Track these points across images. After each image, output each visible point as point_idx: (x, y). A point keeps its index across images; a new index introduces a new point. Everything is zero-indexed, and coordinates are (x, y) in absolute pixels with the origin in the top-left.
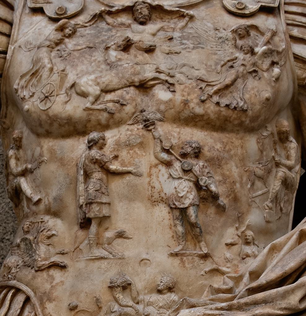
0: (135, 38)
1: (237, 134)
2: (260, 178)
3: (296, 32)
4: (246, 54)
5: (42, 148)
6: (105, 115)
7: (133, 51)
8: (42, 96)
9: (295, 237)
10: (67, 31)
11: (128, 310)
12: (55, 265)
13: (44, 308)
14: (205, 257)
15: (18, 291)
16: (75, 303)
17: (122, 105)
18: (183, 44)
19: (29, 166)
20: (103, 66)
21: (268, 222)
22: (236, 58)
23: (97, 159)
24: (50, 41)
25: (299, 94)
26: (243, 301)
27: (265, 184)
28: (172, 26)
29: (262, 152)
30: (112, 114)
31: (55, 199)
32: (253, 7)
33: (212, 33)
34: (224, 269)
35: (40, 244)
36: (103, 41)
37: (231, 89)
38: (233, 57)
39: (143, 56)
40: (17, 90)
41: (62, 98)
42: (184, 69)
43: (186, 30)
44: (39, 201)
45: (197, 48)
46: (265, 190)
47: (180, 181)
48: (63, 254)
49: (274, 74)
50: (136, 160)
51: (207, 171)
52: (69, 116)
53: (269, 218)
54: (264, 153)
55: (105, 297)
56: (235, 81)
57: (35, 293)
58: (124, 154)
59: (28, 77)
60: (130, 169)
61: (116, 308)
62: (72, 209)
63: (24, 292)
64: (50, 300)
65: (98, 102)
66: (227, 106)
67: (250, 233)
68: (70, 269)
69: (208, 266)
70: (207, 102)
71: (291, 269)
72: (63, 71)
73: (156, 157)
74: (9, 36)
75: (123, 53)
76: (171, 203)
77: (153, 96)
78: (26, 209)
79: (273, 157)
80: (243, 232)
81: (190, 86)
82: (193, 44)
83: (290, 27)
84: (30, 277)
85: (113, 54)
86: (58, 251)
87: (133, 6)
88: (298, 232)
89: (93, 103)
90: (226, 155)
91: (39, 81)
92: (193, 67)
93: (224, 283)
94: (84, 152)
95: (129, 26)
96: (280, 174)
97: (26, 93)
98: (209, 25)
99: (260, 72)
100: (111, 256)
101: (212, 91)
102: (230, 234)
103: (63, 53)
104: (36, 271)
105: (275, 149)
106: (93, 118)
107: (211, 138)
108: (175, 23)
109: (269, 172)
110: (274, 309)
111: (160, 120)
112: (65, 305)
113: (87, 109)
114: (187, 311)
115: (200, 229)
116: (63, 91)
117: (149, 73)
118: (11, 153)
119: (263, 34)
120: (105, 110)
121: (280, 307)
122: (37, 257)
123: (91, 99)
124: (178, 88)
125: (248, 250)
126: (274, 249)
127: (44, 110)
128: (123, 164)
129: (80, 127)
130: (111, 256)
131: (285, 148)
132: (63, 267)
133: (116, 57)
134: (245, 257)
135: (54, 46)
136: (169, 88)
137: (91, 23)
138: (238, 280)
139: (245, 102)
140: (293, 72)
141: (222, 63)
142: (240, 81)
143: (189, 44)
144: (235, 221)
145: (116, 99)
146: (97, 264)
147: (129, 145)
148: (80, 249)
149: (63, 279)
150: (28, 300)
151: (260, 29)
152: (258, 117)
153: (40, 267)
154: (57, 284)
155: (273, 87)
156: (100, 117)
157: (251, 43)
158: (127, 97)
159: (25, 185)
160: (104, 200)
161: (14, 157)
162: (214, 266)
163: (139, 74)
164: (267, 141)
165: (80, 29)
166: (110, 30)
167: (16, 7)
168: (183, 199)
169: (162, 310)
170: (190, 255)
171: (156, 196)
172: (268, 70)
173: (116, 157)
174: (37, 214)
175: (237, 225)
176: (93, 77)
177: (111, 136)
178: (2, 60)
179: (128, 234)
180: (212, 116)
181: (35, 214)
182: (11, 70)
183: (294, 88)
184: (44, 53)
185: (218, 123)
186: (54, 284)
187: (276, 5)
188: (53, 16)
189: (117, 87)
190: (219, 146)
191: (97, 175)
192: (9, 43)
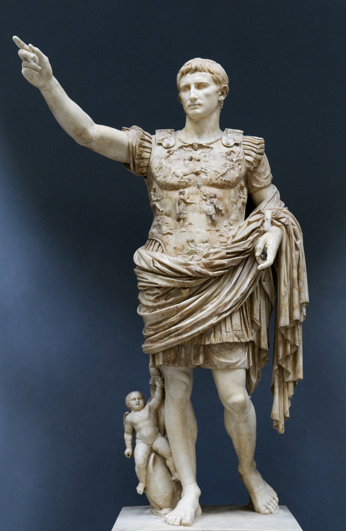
0: (194, 156)
1: (228, 189)
3: (246, 152)
4: (230, 161)
5: (163, 193)
6: (185, 183)
7: (193, 160)
8: (164, 176)
9: (246, 224)
10: (171, 153)
12: (169, 233)
13: (165, 248)
14: (217, 231)
15: (156, 241)
16: (176, 246)
17: (190, 180)
18: (209, 158)
19: (159, 199)
20: (184, 166)
21: (237, 217)
22: (227, 163)
23: (182, 199)
24: (165, 156)
25: (247, 172)
26: (230, 246)
27: (236, 205)
28: (206, 151)
29: (235, 194)
30: (187, 183)
31: (168, 211)
33: (219, 154)
34: (224, 234)
35: (163, 226)
36: (183, 157)
37: (225, 175)
38: (226, 163)
39: (196, 162)
40: (154, 173)
41: (170, 177)
42: (210, 167)
43: (210, 153)
44: (163, 211)
45: (214, 159)
46: (236, 207)
47: (210, 206)
48: (171, 229)
49: (239, 168)
50: (195, 199)
51: (218, 202)
52: (173, 183)
53: (238, 216)
54: (236, 194)
55: (185, 244)
56: (227, 171)
57: (162, 242)
58: (191, 197)
59: (158, 169)
60: (193, 202)
61: (189, 248)
62: (174, 214)
63: (158, 242)
64: (167, 245)
65: (182, 179)
66: (225, 181)
67: (232, 222)
68: (174, 235)
69: (219, 234)
70: (218, 179)
71: (245, 235)
72: (170, 168)
73: (202, 198)
74: (151, 153)
75: (190, 161)
76: (207, 213)
77: (200, 177)
78: (157, 212)
79: (239, 195)
80: (230, 222)
81: (212, 174)
82: (213, 158)
83: (244, 150)
84: (160, 237)
85: (187, 162)
86: (170, 228)
87: (193, 144)
88: (247, 222)
89: (181, 179)
90: (224, 197)
91: (162, 171)
92: (213, 167)
93: (224, 240)
94: (178, 196)
95: (191, 151)
96: (241, 201)
97: (157, 175)
98: (219, 151)
99: (235, 168)
100: (187, 231)
101: (220, 175)
102: (226, 223)
103: (170, 161)
104: (163, 235)
105: (240, 192)
106: (181, 184)
107: (219, 191)
108: (206, 150)
109: (238, 200)
110: (240, 248)
111: (203, 185)
112: (173, 246)
113: (179, 182)
114: (213, 249)
115: (216, 221)
116: (170, 175)
117: (198, 169)
118: (152, 193)
119: (235, 153)
120: (185, 182)
121: (242, 248)
122: (163, 230)
123: (180, 178)
124: (208, 174)
125: (231, 227)
126: (240, 227)
127: (164, 181)
128: (191, 200)
129: (176, 187)
130: (187, 231)
131: (243, 191)
132: (171, 234)
133: (188, 163)
135: (166, 157)
136: (205, 174)
137: (178, 150)
138: (228, 238)
139: (230, 179)
140: (245, 166)
141: (223, 165)
142: (228, 171)
143: (211, 158)
144: (227, 218)
145: (188, 178)
146: (183, 233)
147: (193, 194)
148: (177, 228)
149: (172, 238)
150: (160, 244)
151: (235, 152)
152: (234, 183)
153: (164, 234)
154: (169, 240)
155: (239, 173)
156: (183, 184)
157: (232, 158)
158: (192, 177)
159: (158, 205)
160: (185, 212)
161: (153, 195)
162: (221, 234)
163: (195, 169)
164: (237, 190)
165: (175, 152)
166: (185, 153)
167: (152, 143)
168: (210, 212)
169: (204, 249)
170: (213, 230)
171: (202, 211)
172: (237, 167)
173: (188, 198)
174: (162, 215)
175: (228, 219)
176: (180, 170)
177: (187, 190)
178: (149, 161)
179: (192, 224)
180: (220, 184)
181: (161, 215)
182: (152, 165)
183: (246, 171)
185: (221, 186)
186: (169, 239)
187: (240, 143)
188: (166, 147)
189: (188, 174)
190: (222, 194)
191: (183, 204)
192: (151, 156)
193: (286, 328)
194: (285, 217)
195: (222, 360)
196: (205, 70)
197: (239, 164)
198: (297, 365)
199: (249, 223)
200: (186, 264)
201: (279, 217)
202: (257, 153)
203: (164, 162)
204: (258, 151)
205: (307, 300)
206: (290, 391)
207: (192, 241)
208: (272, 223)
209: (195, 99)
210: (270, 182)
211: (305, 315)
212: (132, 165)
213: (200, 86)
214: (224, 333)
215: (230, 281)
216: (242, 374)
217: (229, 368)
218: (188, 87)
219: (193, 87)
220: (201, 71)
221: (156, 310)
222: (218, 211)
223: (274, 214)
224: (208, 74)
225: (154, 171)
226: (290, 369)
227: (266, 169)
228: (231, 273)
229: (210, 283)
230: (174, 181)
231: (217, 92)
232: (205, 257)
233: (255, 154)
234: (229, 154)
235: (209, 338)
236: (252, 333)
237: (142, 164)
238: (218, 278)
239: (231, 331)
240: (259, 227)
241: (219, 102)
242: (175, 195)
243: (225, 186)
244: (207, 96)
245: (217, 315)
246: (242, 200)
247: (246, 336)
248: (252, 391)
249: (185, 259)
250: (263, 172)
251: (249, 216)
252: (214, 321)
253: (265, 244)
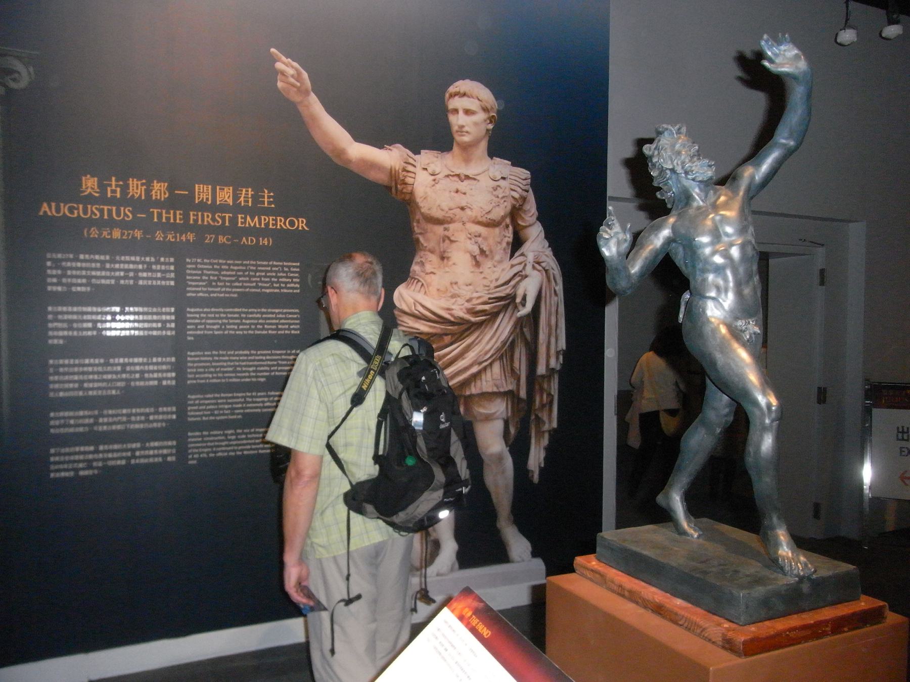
0: (460, 188)
2: (499, 243)
3: (513, 187)
7: (459, 193)
11: (457, 292)
14: (481, 273)
15: (415, 279)
30: (452, 219)
34: (487, 277)
55: (448, 284)
61: (452, 290)
69: (483, 276)
109: (502, 240)
117: (464, 204)
120: (450, 217)
125: (495, 269)
126: (503, 270)
134: (494, 272)
177: (452, 226)
190: (486, 233)
191: (447, 241)
193: (543, 376)
195: (482, 410)
197: (505, 201)
198: (552, 414)
200: (448, 309)
202: (523, 190)
204: (524, 188)
205: (564, 348)
206: (545, 441)
207: (456, 283)
209: (463, 127)
210: (535, 219)
211: (562, 362)
213: (468, 112)
214: (484, 383)
215: (492, 327)
216: (499, 425)
217: (488, 418)
218: (456, 111)
219: (461, 112)
220: (469, 97)
222: (482, 252)
226: (545, 418)
227: (531, 207)
229: (472, 329)
230: (438, 214)
231: (485, 121)
232: (468, 301)
233: (521, 190)
234: (495, 189)
235: (470, 389)
236: (511, 382)
238: (479, 325)
239: (491, 380)
241: (488, 130)
243: (491, 224)
246: (506, 239)
247: (505, 385)
248: (510, 443)
250: (529, 210)
251: (514, 255)
252: (475, 369)
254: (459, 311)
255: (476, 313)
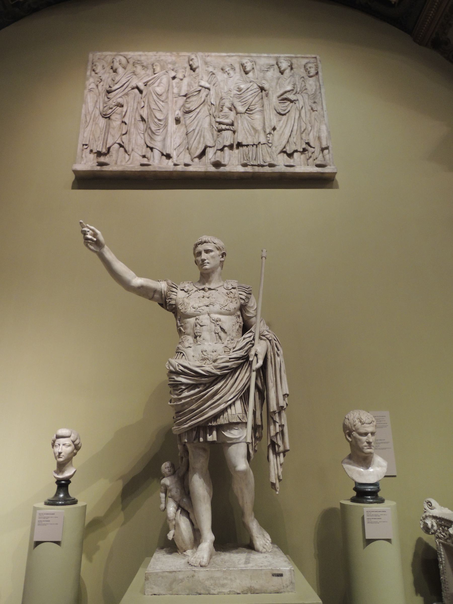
10: (190, 294)
11: (206, 357)
14: (223, 343)
15: (181, 353)
32: (230, 287)
41: (189, 309)
61: (203, 356)
109: (236, 324)
116: (189, 307)
125: (232, 341)
130: (201, 344)
138: (230, 349)
151: (233, 292)
159: (182, 329)
177: (201, 317)
184: (185, 299)
188: (186, 291)
191: (198, 326)
194: (269, 334)
196: (210, 241)
199: (244, 339)
201: (265, 334)
202: (247, 294)
203: (185, 299)
208: (261, 339)
209: (205, 260)
212: (164, 305)
213: (207, 251)
221: (181, 401)
223: (261, 333)
224: (213, 244)
225: (179, 306)
228: (233, 373)
229: (219, 379)
237: (171, 303)
240: (251, 341)
242: (192, 320)
244: (213, 257)
245: (225, 402)
249: (201, 364)
252: (222, 407)
253: (256, 352)
254: (209, 367)
255: (221, 368)
